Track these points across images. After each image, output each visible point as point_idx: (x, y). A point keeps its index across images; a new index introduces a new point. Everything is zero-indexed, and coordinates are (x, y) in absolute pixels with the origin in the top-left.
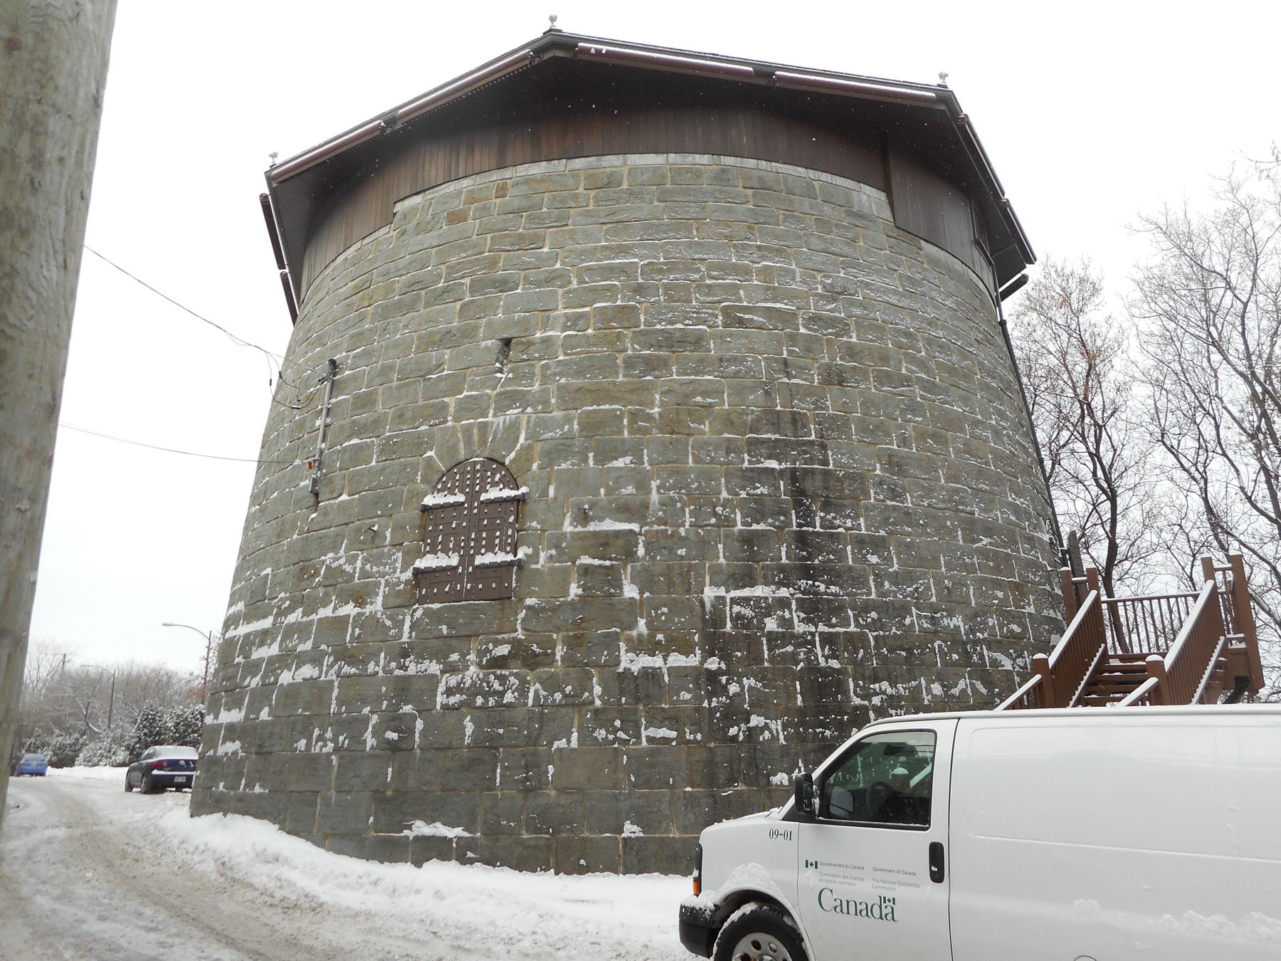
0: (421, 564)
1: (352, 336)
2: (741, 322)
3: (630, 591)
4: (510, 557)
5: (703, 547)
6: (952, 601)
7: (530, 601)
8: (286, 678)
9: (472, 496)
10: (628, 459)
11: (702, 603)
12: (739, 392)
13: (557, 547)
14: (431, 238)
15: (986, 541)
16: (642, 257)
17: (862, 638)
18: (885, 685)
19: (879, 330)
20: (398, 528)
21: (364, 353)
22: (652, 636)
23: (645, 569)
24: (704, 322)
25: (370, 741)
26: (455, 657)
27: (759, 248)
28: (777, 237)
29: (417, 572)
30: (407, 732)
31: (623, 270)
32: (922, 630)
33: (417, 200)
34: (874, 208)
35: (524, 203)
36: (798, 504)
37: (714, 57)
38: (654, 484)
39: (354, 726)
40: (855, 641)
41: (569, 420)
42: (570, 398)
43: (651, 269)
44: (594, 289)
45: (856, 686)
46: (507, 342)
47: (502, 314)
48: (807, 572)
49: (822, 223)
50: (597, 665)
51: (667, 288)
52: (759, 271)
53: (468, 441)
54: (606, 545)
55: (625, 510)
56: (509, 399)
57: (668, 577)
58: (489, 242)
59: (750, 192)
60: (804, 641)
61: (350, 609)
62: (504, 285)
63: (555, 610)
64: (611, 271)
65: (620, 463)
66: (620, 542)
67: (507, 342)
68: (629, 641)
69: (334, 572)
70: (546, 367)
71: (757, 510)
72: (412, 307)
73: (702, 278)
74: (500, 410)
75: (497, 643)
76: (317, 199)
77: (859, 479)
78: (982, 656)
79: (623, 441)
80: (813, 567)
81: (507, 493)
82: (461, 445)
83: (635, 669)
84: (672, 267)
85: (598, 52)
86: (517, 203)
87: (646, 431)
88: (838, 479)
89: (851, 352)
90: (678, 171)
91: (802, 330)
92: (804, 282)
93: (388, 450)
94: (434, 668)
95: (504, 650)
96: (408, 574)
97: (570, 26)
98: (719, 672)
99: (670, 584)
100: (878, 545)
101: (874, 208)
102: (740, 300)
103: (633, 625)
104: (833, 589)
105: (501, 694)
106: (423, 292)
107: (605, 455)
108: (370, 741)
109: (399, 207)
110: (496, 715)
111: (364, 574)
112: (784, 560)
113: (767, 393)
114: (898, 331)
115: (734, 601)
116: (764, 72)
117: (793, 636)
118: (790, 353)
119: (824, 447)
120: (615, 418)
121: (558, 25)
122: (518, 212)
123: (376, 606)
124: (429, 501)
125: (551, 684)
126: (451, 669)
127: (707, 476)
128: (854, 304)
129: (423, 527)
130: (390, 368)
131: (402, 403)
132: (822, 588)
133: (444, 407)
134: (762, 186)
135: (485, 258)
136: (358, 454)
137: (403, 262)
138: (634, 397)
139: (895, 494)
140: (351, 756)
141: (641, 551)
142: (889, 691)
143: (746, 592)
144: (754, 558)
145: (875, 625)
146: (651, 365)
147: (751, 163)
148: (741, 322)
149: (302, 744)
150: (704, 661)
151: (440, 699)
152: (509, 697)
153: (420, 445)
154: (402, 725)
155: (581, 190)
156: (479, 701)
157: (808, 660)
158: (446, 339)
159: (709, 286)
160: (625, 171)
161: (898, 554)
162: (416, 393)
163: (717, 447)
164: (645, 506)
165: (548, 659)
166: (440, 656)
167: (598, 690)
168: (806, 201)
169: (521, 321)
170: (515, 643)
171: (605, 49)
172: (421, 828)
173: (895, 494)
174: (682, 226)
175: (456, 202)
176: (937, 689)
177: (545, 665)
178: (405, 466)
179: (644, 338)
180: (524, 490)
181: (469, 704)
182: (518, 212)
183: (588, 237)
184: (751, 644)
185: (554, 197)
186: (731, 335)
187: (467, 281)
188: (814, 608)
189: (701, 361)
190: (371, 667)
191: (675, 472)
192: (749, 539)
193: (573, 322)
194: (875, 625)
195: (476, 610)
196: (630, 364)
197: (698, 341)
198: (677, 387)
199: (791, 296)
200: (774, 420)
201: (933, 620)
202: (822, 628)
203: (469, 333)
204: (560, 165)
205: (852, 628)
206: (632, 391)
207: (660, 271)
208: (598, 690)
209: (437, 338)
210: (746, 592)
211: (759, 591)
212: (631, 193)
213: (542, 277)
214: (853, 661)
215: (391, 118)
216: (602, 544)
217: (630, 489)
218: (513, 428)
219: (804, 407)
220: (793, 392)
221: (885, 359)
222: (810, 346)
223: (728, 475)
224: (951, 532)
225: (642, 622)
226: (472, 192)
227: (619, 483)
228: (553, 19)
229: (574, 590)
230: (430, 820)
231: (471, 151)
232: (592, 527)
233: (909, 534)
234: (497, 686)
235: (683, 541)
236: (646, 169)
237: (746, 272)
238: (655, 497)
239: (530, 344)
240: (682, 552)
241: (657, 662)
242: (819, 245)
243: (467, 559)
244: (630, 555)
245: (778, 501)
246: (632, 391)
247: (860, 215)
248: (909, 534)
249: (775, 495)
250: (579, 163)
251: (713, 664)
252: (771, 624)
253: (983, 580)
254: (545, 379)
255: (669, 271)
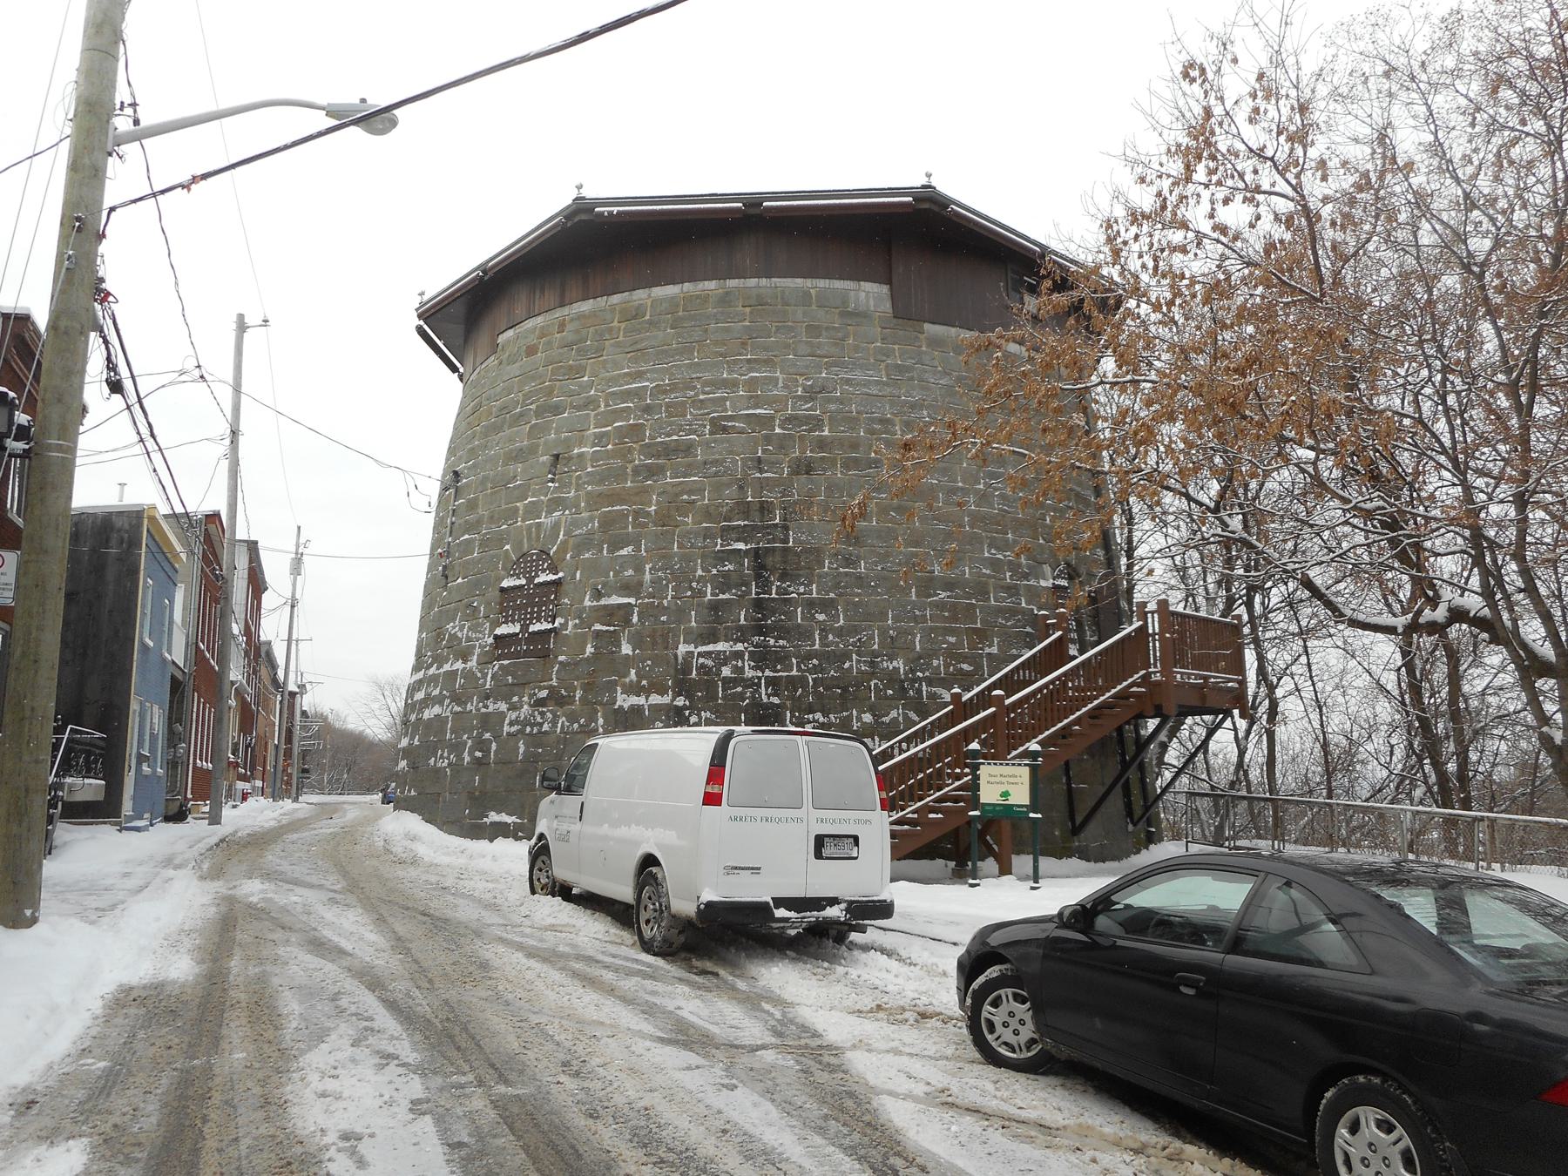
0: (498, 631)
2: (725, 430)
3: (626, 649)
4: (550, 626)
5: (680, 614)
6: (893, 647)
7: (561, 658)
8: (427, 714)
9: (530, 580)
10: (630, 548)
11: (676, 656)
12: (717, 489)
13: (580, 617)
14: (514, 369)
15: (943, 595)
16: (652, 381)
17: (802, 681)
18: (818, 716)
19: (853, 422)
20: (488, 604)
21: (474, 466)
22: (639, 682)
23: (638, 632)
24: (695, 432)
25: (467, 759)
26: (515, 699)
27: (749, 361)
28: (766, 349)
29: (496, 637)
30: (487, 752)
31: (638, 394)
32: (863, 673)
33: (510, 333)
34: (872, 302)
36: (758, 577)
37: (714, 198)
38: (648, 567)
39: (457, 748)
40: (793, 683)
41: (591, 519)
42: (595, 501)
43: (659, 390)
44: (614, 411)
45: (792, 716)
48: (761, 630)
49: (814, 330)
50: (601, 704)
51: (668, 406)
52: (745, 381)
54: (611, 615)
55: (628, 588)
56: (556, 504)
57: (652, 636)
59: (748, 310)
60: (753, 684)
61: (459, 665)
62: (557, 410)
63: (576, 664)
64: (627, 396)
65: (624, 552)
66: (622, 612)
67: (557, 457)
68: (623, 686)
69: (453, 637)
70: (579, 477)
71: (724, 583)
73: (697, 395)
74: (549, 513)
75: (541, 689)
76: (462, 318)
77: (816, 554)
78: (919, 691)
80: (766, 626)
81: (552, 577)
83: (626, 706)
84: (674, 387)
85: (611, 213)
87: (644, 525)
88: (796, 554)
89: (822, 444)
90: (689, 299)
91: (778, 430)
92: (785, 387)
93: (484, 544)
94: (503, 706)
95: (544, 694)
96: (491, 640)
98: (685, 707)
99: (654, 643)
100: (826, 605)
101: (872, 302)
102: (726, 410)
103: (627, 674)
104: (781, 642)
105: (541, 725)
107: (615, 547)
108: (467, 759)
109: (501, 339)
110: (537, 739)
111: (469, 639)
112: (742, 622)
113: (741, 488)
114: (872, 420)
115: (700, 655)
116: (753, 202)
117: (743, 680)
118: (764, 451)
119: (786, 528)
120: (623, 516)
123: (473, 663)
124: (505, 584)
125: (572, 718)
126: (513, 708)
127: (687, 559)
128: (829, 400)
129: (501, 604)
132: (772, 642)
134: (759, 303)
136: (467, 547)
137: (498, 389)
138: (637, 499)
139: (849, 561)
140: (456, 767)
141: (635, 619)
142: (821, 719)
143: (710, 648)
144: (718, 620)
145: (815, 670)
146: (653, 472)
147: (752, 282)
148: (725, 430)
149: (432, 761)
150: (674, 699)
151: (506, 728)
152: (546, 727)
153: (501, 540)
154: (481, 745)
155: (615, 323)
156: (528, 729)
157: (753, 697)
158: (518, 456)
159: (702, 401)
161: (845, 612)
163: (697, 535)
164: (640, 584)
165: (570, 700)
166: (507, 698)
167: (601, 721)
168: (800, 310)
170: (551, 688)
171: (615, 210)
172: (494, 817)
173: (849, 561)
174: (686, 350)
176: (867, 718)
178: (493, 556)
179: (649, 450)
180: (561, 575)
181: (521, 732)
183: (617, 365)
184: (710, 687)
186: (715, 441)
187: (533, 407)
188: (763, 658)
189: (689, 465)
190: (469, 707)
191: (664, 557)
192: (715, 606)
193: (600, 439)
194: (815, 670)
195: (528, 664)
196: (636, 471)
197: (688, 449)
199: (769, 402)
200: (744, 509)
201: (872, 664)
202: (768, 673)
203: (533, 450)
204: (602, 302)
205: (794, 673)
207: (665, 392)
208: (601, 721)
210: (710, 648)
211: (721, 646)
212: (650, 322)
214: (792, 698)
215: (483, 268)
216: (609, 614)
217: (630, 572)
218: (556, 527)
219: (771, 497)
220: (762, 484)
221: (854, 446)
222: (783, 444)
223: (703, 557)
224: (905, 591)
225: (633, 672)
227: (623, 568)
228: (579, 187)
229: (589, 649)
230: (499, 812)
231: (543, 292)
232: (603, 602)
233: (858, 595)
234: (539, 719)
235: (665, 610)
237: (734, 384)
238: (647, 577)
239: (570, 458)
240: (664, 618)
241: (641, 700)
242: (803, 349)
243: (525, 628)
244: (627, 622)
245: (742, 575)
247: (855, 314)
248: (858, 595)
249: (739, 571)
250: (616, 299)
251: (680, 701)
252: (726, 671)
253: (932, 629)
255: (672, 391)
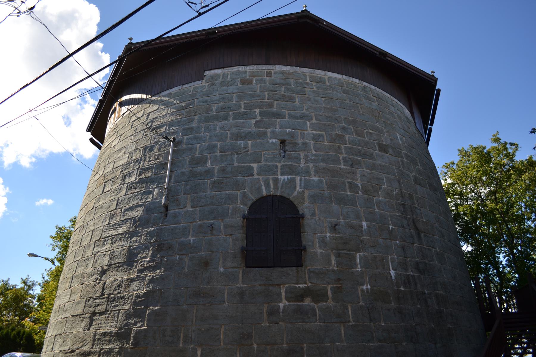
1: (184, 129)
35: (282, 81)
46: (283, 142)
47: (279, 128)
53: (267, 185)
58: (267, 95)
59: (375, 98)
72: (225, 118)
79: (347, 195)
82: (263, 188)
86: (278, 81)
97: (316, 11)
106: (231, 113)
109: (207, 73)
121: (308, 9)
122: (280, 85)
130: (215, 146)
131: (224, 164)
133: (251, 168)
135: (266, 102)
155: (308, 81)
158: (248, 136)
160: (326, 78)
162: (232, 160)
169: (289, 133)
175: (244, 75)
177: (323, 301)
182: (280, 85)
185: (297, 82)
198: (366, 174)
206: (348, 173)
209: (243, 135)
213: (298, 115)
226: (253, 72)
236: (335, 79)
246: (348, 173)
250: (305, 70)
254: (306, 161)
